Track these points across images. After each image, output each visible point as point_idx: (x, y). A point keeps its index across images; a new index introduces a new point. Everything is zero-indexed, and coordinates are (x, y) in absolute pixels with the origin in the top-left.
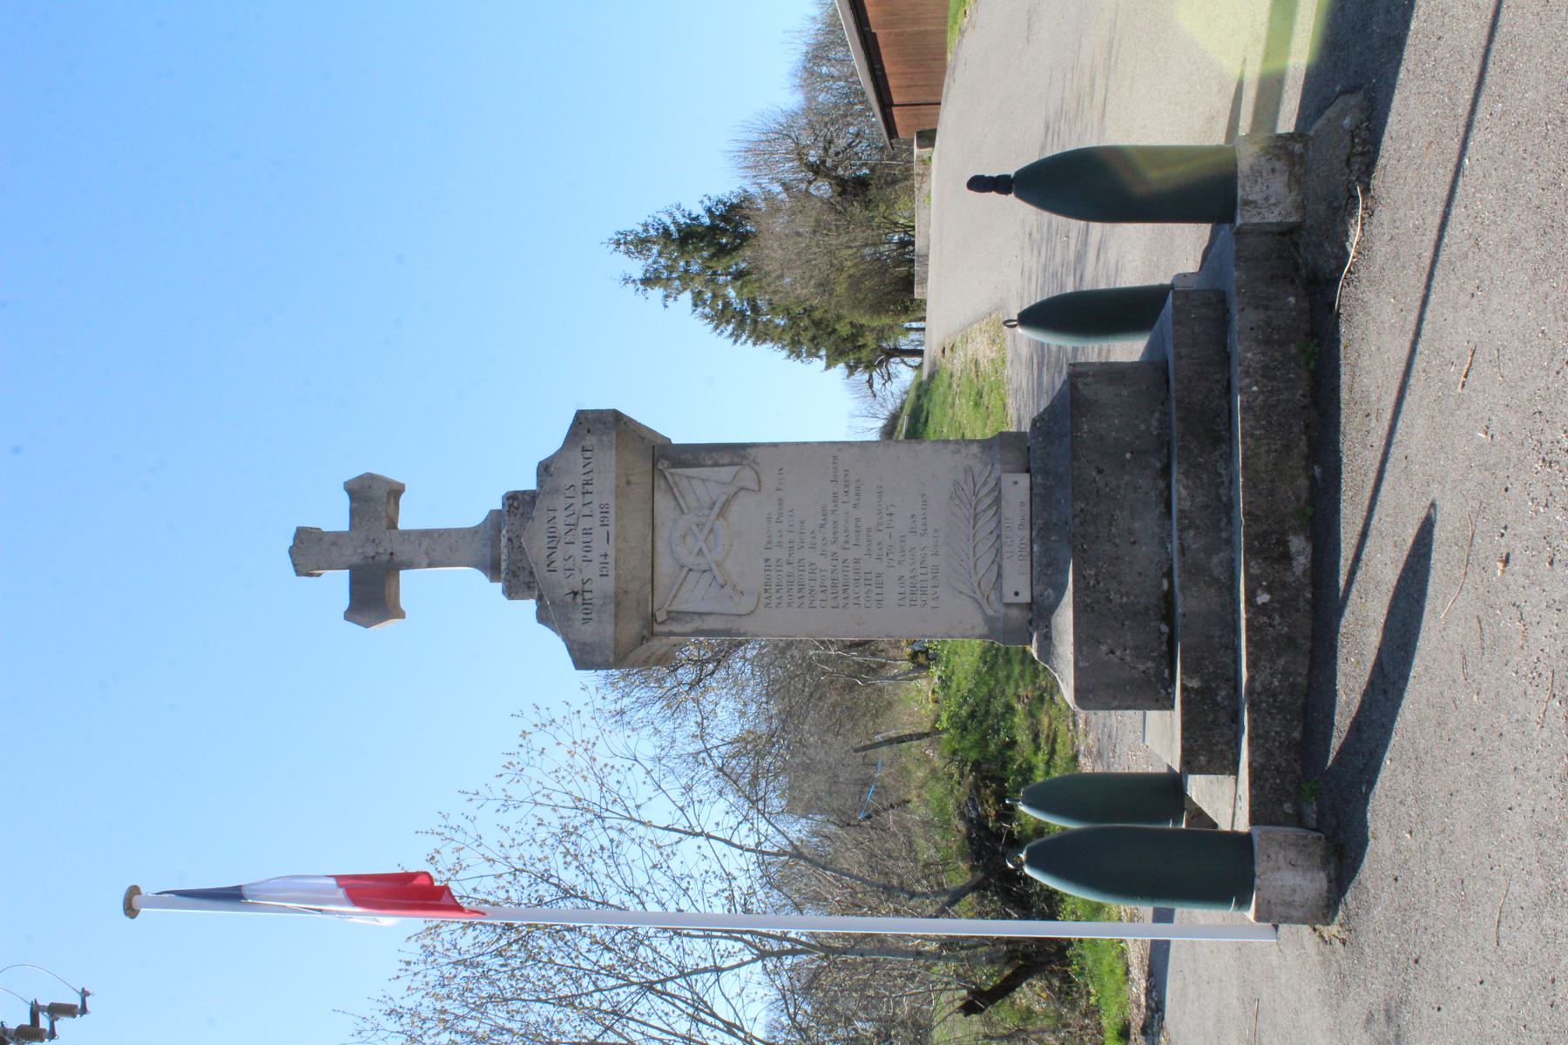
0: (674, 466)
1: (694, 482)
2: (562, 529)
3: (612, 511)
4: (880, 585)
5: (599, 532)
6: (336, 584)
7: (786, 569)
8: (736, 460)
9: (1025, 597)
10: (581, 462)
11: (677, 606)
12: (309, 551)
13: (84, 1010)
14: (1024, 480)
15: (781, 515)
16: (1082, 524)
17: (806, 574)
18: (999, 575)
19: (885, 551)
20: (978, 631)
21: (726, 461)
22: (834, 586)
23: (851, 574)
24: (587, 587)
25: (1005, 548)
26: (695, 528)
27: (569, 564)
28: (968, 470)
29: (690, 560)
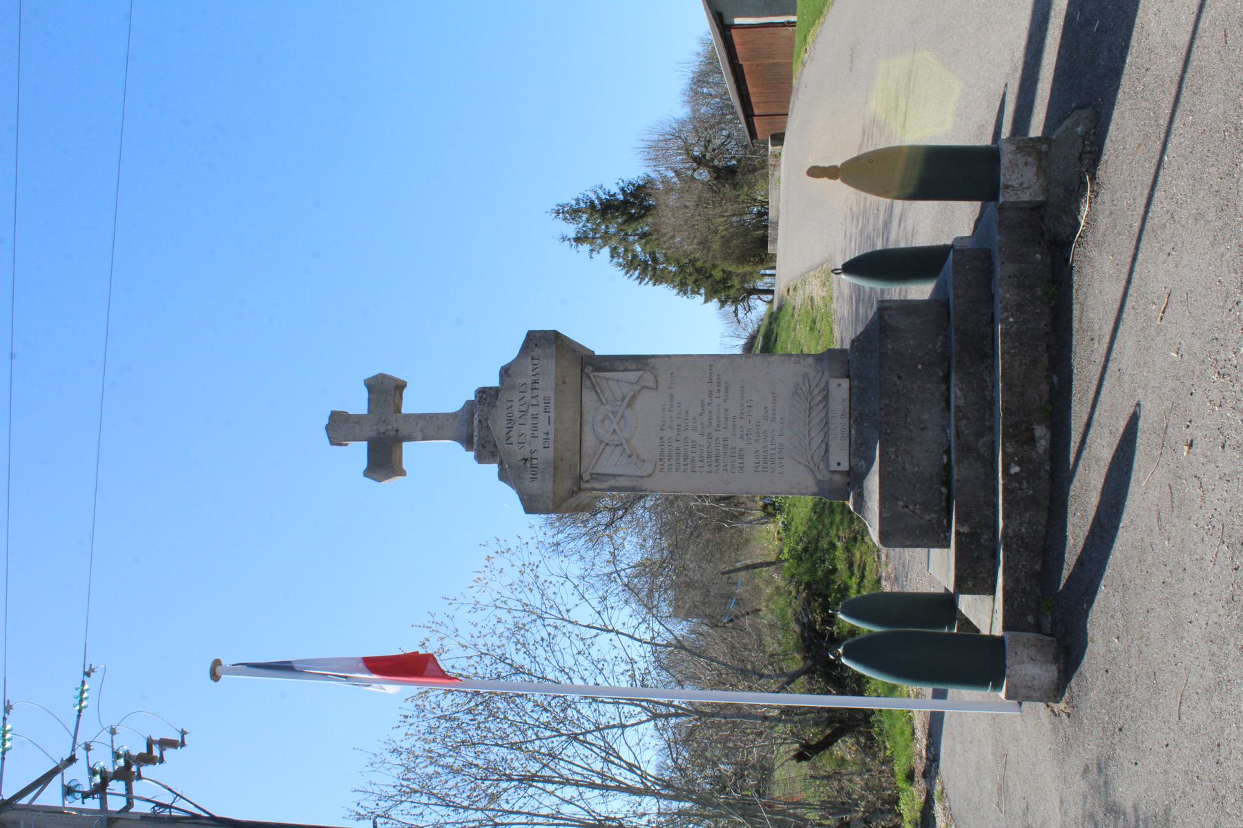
2: (517, 414)
3: (552, 401)
4: (741, 457)
5: (543, 417)
6: (358, 451)
7: (675, 444)
9: (845, 466)
10: (531, 367)
11: (599, 469)
12: (340, 428)
13: (183, 744)
14: (845, 383)
18: (827, 451)
24: (534, 455)
25: (831, 432)
27: (522, 439)
28: (806, 376)
29: (608, 437)
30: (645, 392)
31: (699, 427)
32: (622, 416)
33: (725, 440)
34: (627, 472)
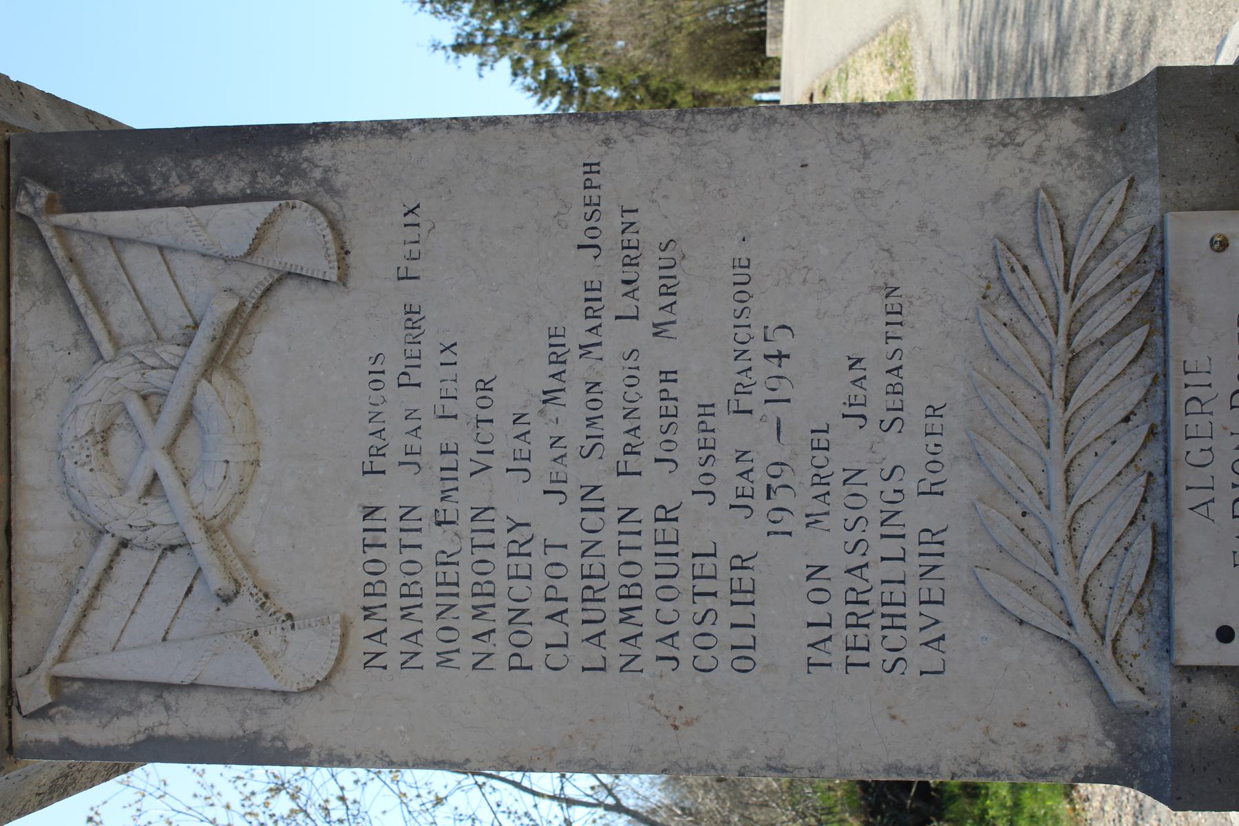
0: (71, 207)
4: (743, 596)
7: (434, 540)
8: (266, 180)
11: (84, 665)
15: (414, 360)
17: (498, 556)
19: (760, 479)
20: (1078, 756)
21: (237, 182)
22: (591, 598)
23: (645, 557)
25: (1182, 476)
28: (1043, 205)
29: (122, 512)
30: (289, 290)
31: (542, 461)
32: (189, 414)
33: (666, 515)
34: (213, 673)
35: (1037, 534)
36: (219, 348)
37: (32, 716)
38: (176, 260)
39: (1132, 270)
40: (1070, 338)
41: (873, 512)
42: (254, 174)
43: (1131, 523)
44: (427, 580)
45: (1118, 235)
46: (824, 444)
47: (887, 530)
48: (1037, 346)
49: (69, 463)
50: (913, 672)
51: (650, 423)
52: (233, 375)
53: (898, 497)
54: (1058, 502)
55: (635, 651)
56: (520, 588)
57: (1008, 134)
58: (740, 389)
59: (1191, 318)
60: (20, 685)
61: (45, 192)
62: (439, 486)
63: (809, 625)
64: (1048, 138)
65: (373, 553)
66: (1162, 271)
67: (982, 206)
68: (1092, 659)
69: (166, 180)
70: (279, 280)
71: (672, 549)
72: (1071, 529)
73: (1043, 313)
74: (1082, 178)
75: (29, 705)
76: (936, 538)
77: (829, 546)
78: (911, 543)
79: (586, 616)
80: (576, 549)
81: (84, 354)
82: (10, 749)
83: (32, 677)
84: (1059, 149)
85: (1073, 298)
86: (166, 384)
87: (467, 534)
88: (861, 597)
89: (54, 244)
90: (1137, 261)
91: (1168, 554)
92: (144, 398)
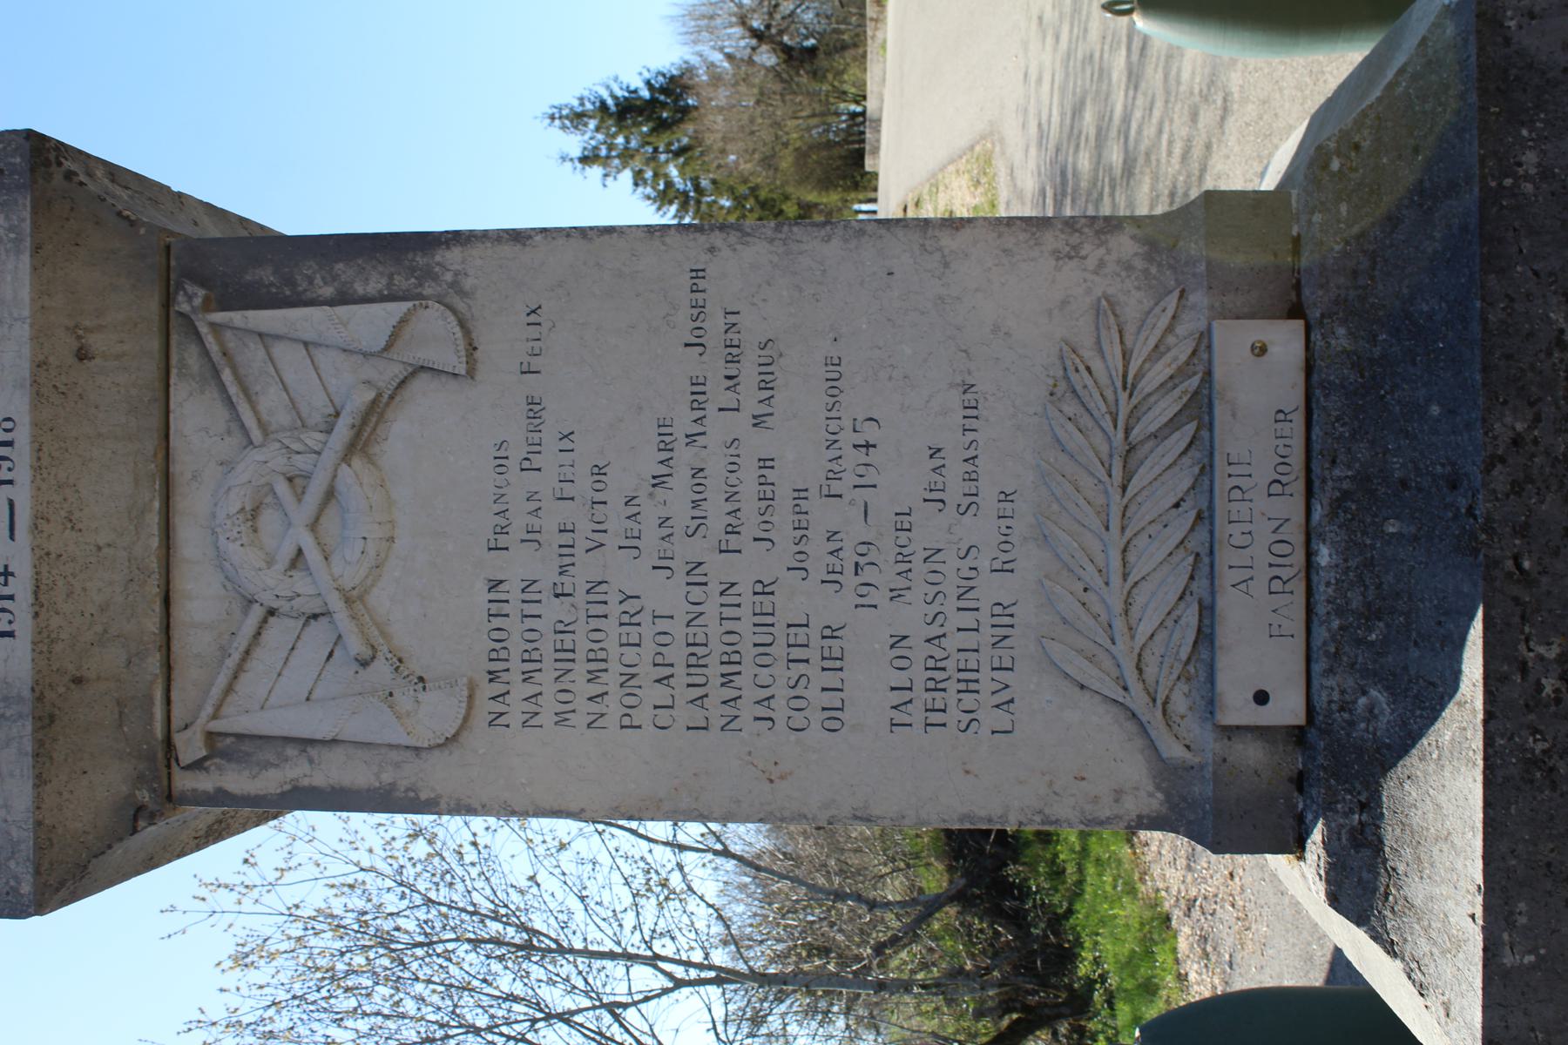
0: (225, 307)
1: (279, 350)
4: (833, 663)
7: (553, 611)
8: (402, 283)
9: (1288, 709)
11: (236, 721)
14: (1286, 340)
15: (535, 447)
16: (1517, 488)
17: (611, 625)
19: (849, 557)
20: (1131, 807)
21: (375, 284)
23: (745, 627)
25: (1225, 557)
26: (282, 488)
29: (270, 583)
30: (421, 383)
31: (651, 536)
32: (330, 494)
34: (353, 728)
35: (1097, 608)
36: (358, 434)
37: (189, 767)
38: (319, 355)
39: (1182, 373)
40: (1127, 432)
41: (951, 587)
42: (391, 277)
43: (1181, 598)
44: (546, 648)
45: (1171, 340)
46: (906, 526)
47: (963, 604)
48: (1098, 439)
49: (222, 539)
50: (985, 731)
51: (750, 506)
52: (371, 460)
53: (973, 574)
54: (1116, 579)
55: (736, 713)
56: (630, 655)
57: (1074, 248)
58: (831, 475)
59: (1234, 415)
60: (178, 739)
61: (201, 292)
62: (558, 561)
63: (893, 689)
64: (1109, 252)
65: (497, 622)
66: (1209, 373)
67: (1050, 312)
68: (1144, 719)
69: (311, 281)
70: (413, 374)
71: (769, 620)
72: (1127, 604)
73: (1104, 409)
74: (1138, 288)
75: (186, 757)
76: (1008, 611)
77: (911, 617)
78: (984, 616)
79: (691, 680)
80: (682, 619)
81: (236, 440)
82: (169, 798)
83: (188, 733)
84: (1118, 262)
85: (1131, 396)
86: (309, 468)
87: (582, 605)
88: (939, 665)
89: (210, 340)
90: (1187, 363)
91: (1212, 626)
92: (290, 480)
